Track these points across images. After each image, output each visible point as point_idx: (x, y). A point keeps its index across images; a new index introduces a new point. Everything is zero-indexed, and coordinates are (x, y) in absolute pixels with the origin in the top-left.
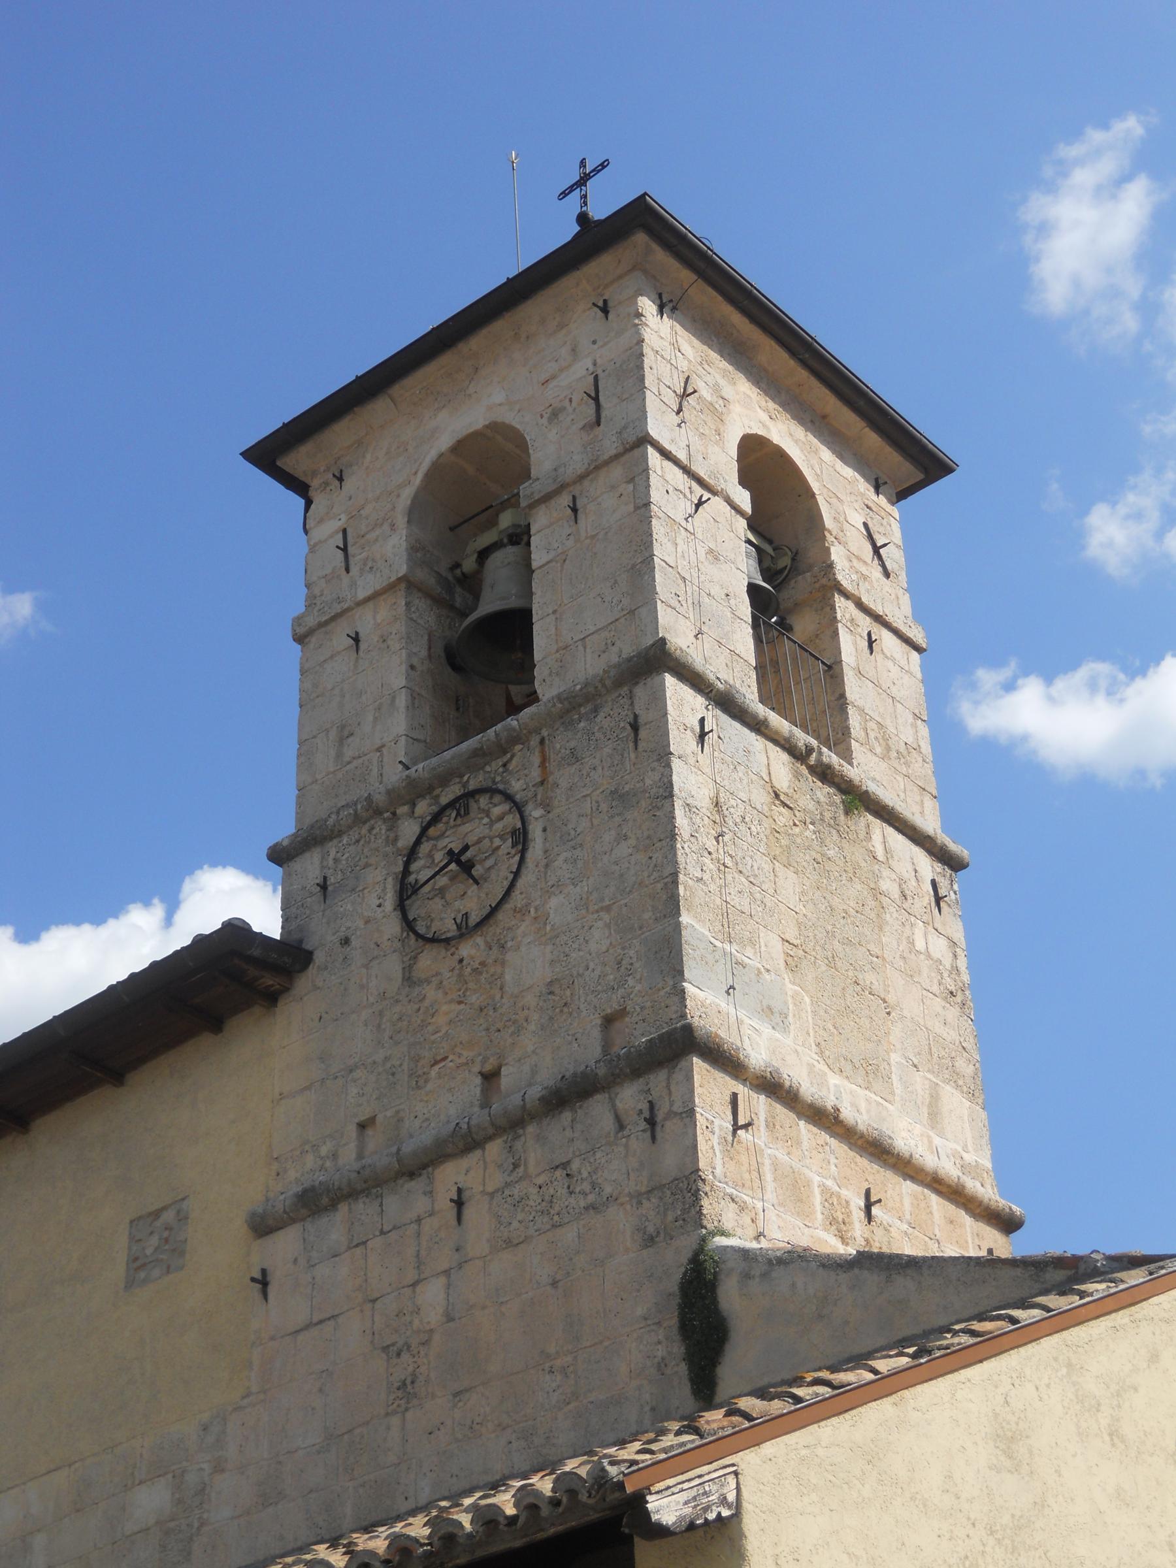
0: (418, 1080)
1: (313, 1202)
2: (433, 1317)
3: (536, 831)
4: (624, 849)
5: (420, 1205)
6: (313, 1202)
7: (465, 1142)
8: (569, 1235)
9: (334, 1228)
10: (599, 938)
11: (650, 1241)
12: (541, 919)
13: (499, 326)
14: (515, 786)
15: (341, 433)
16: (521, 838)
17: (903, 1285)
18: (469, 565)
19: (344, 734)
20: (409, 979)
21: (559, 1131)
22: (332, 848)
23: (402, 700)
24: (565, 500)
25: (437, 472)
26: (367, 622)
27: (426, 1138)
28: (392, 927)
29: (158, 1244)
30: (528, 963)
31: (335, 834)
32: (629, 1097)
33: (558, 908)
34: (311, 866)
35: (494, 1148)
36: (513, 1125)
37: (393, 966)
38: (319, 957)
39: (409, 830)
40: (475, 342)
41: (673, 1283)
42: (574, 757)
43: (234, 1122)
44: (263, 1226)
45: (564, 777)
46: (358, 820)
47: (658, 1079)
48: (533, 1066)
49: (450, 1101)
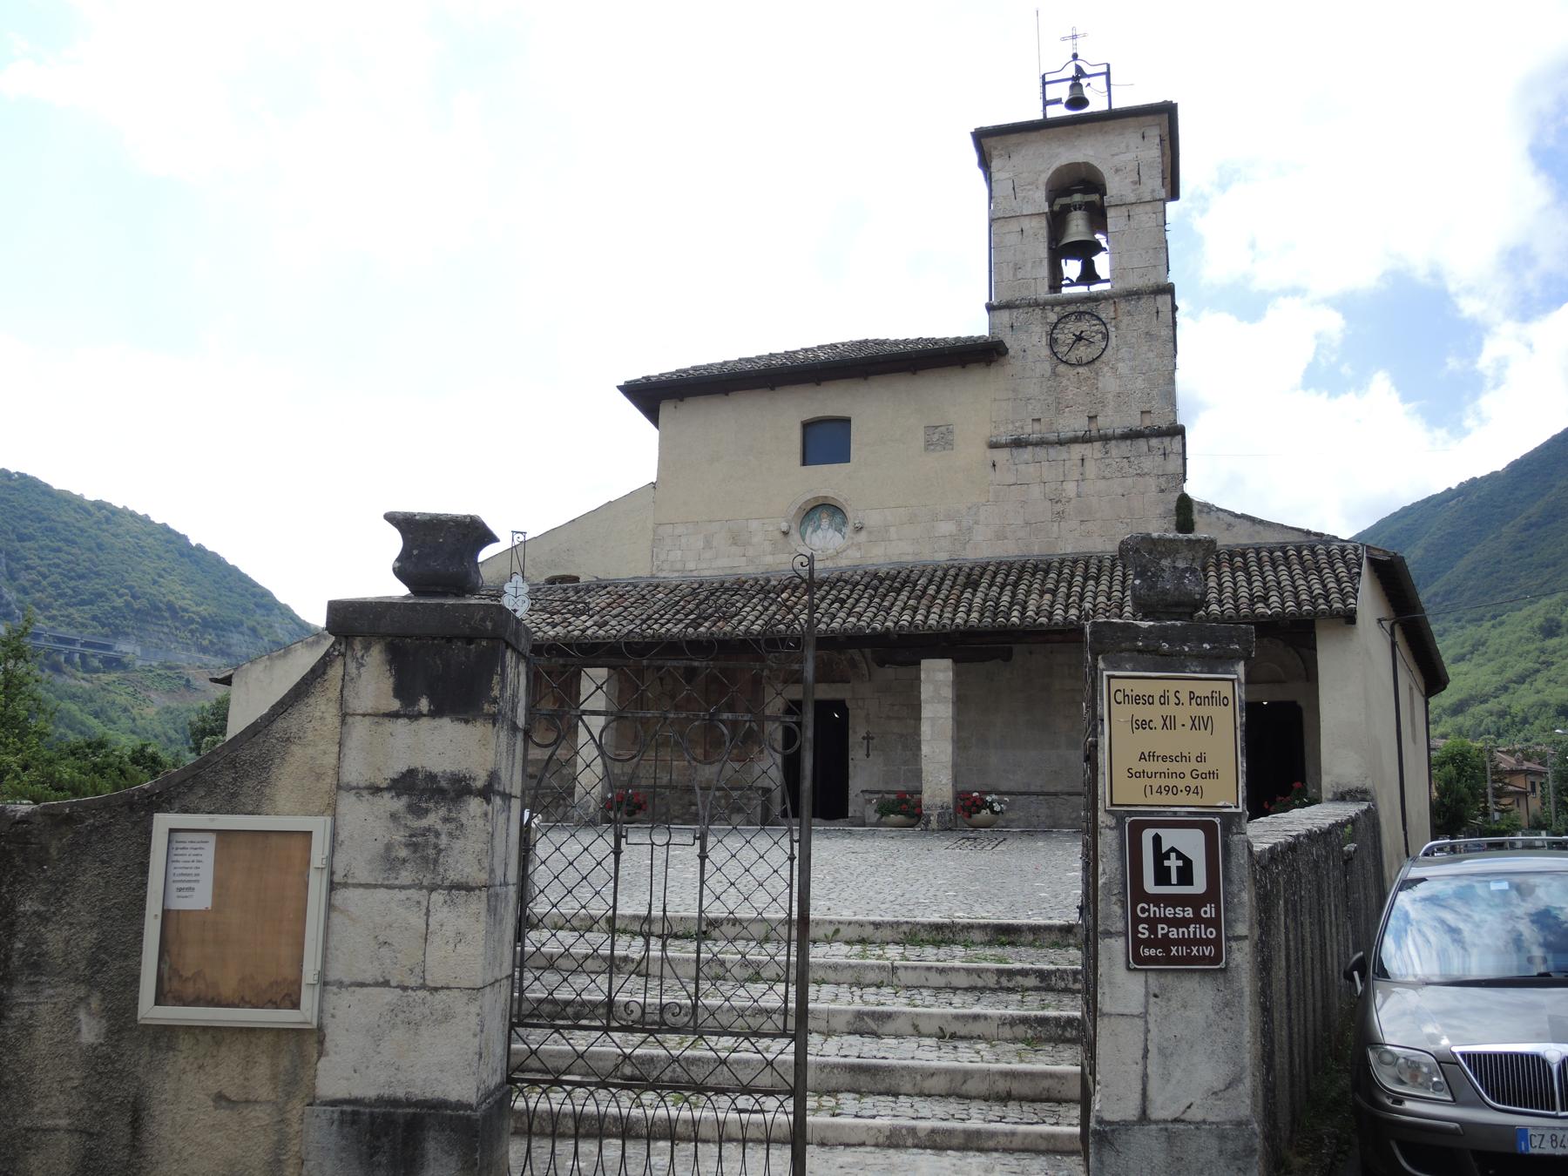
0: (1059, 411)
1: (1018, 443)
2: (1072, 494)
3: (1112, 335)
4: (1151, 355)
5: (1065, 456)
6: (1018, 443)
7: (1086, 439)
8: (1129, 481)
9: (1027, 453)
10: (1140, 383)
11: (1162, 491)
12: (1114, 369)
13: (1097, 125)
14: (1103, 316)
15: (1014, 138)
16: (1106, 337)
17: (1259, 528)
18: (1056, 208)
19: (1017, 268)
20: (1054, 373)
21: (1125, 447)
22: (1015, 312)
23: (1045, 263)
24: (1124, 209)
25: (1058, 171)
26: (1027, 224)
27: (1071, 434)
28: (1046, 352)
29: (939, 438)
30: (1108, 382)
31: (1017, 307)
32: (1154, 442)
33: (1123, 368)
34: (1005, 316)
35: (1098, 445)
36: (1105, 439)
37: (1047, 367)
38: (1011, 352)
39: (1053, 318)
40: (1084, 127)
41: (1173, 506)
42: (1129, 313)
43: (973, 406)
44: (994, 446)
45: (1125, 320)
46: (1029, 305)
47: (1167, 440)
48: (1112, 421)
49: (1074, 423)
